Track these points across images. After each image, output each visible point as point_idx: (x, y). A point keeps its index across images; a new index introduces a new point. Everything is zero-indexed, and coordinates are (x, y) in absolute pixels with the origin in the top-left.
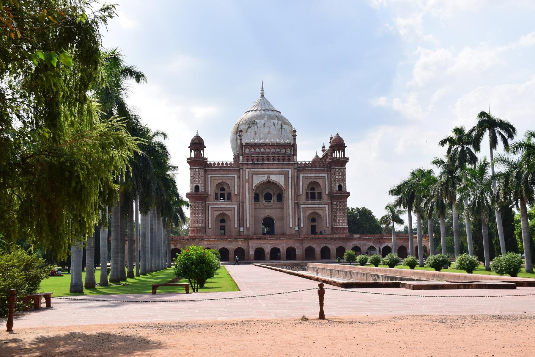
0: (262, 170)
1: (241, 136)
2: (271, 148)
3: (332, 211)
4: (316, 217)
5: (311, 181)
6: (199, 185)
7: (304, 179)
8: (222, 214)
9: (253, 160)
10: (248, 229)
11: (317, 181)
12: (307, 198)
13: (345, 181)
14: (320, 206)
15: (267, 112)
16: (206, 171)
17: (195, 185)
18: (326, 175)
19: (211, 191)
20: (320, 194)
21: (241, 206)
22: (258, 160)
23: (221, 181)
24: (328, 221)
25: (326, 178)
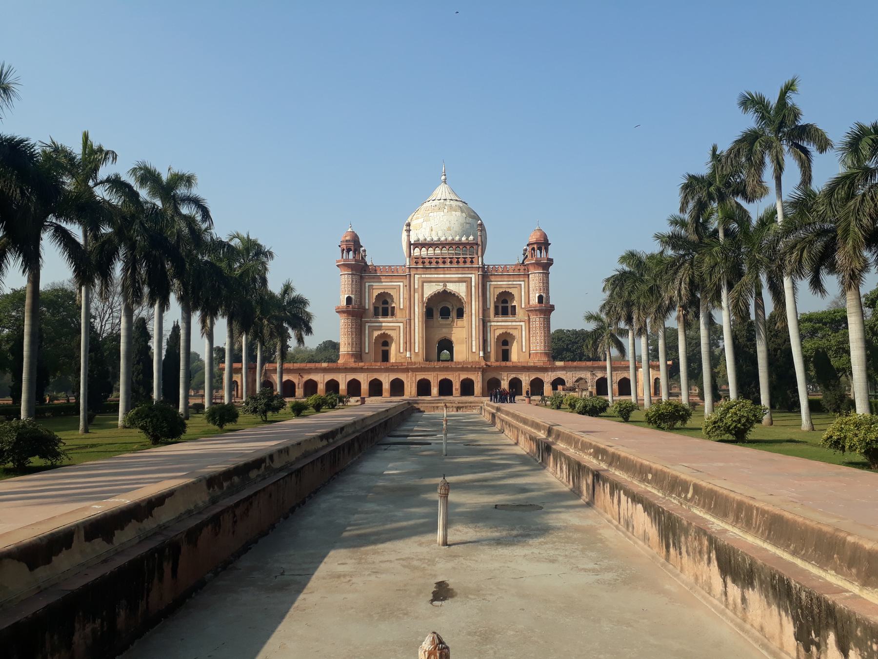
4: (509, 339)
5: (501, 290)
6: (353, 296)
8: (384, 335)
9: (423, 263)
10: (417, 354)
11: (510, 291)
12: (496, 314)
13: (548, 290)
14: (514, 324)
15: (448, 202)
16: (361, 277)
17: (346, 296)
18: (522, 283)
19: (369, 303)
22: (430, 263)
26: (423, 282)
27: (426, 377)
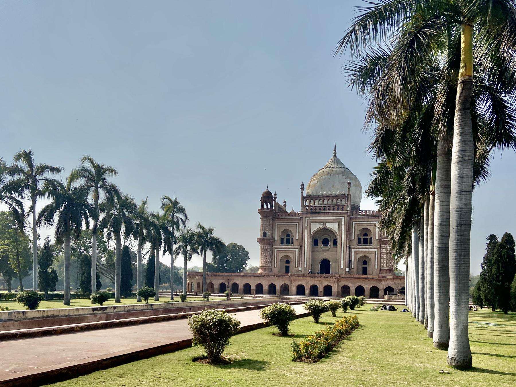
0: (319, 218)
1: (302, 189)
2: (327, 199)
3: (380, 254)
4: (366, 260)
5: (362, 228)
6: (267, 232)
7: (356, 226)
9: (311, 210)
11: (368, 227)
12: (359, 242)
14: (370, 250)
16: (273, 219)
20: (371, 239)
21: (301, 249)
22: (316, 210)
23: (286, 228)
24: (376, 263)
25: (377, 225)
26: (311, 222)
27: (302, 283)
